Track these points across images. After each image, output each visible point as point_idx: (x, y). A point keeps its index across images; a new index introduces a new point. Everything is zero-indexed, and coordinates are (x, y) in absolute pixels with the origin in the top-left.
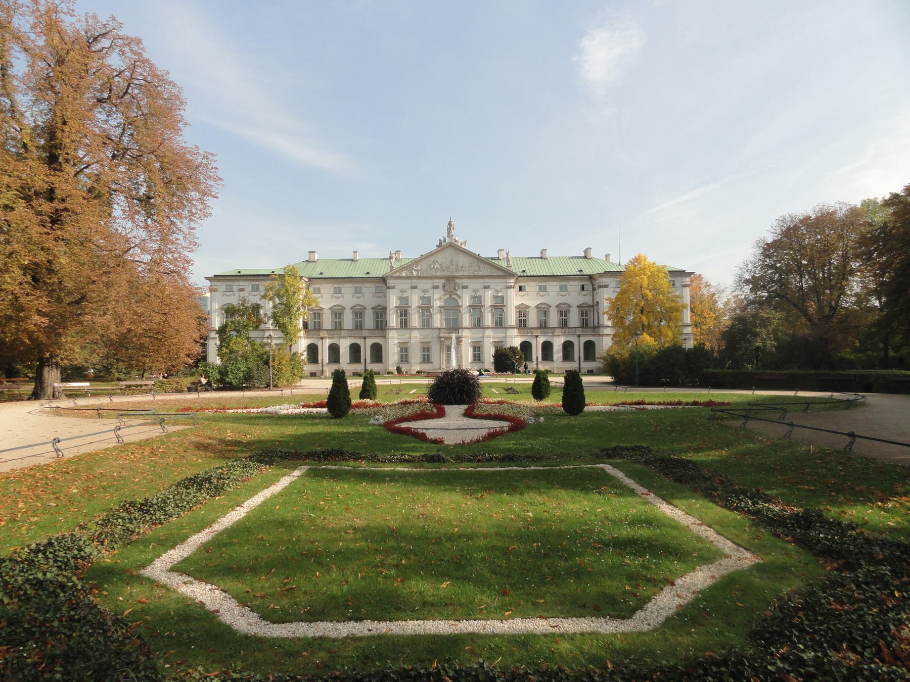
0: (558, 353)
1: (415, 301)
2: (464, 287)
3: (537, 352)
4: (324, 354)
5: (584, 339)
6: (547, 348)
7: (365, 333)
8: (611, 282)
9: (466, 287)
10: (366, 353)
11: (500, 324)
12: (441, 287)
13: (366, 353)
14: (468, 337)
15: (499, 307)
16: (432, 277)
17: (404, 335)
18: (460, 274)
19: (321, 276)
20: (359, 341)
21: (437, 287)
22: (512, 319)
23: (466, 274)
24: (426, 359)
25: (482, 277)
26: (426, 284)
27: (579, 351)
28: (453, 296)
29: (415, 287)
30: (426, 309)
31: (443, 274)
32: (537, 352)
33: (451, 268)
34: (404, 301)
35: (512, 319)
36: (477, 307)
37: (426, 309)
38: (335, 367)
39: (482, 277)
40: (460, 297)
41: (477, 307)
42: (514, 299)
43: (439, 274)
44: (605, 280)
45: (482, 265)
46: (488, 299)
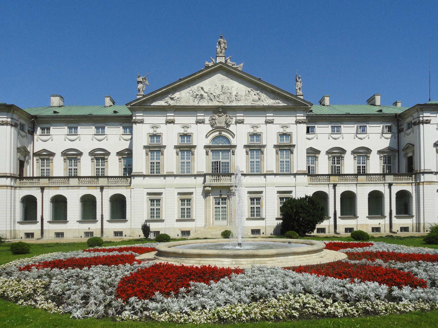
0: (362, 205)
2: (237, 122)
3: (334, 205)
4: (45, 209)
5: (396, 189)
9: (242, 122)
10: (104, 208)
12: (207, 121)
13: (104, 208)
14: (245, 186)
15: (285, 148)
17: (155, 183)
18: (234, 104)
20: (96, 193)
21: (203, 122)
22: (300, 161)
24: (186, 215)
28: (223, 133)
29: (172, 122)
30: (186, 148)
31: (211, 104)
33: (222, 97)
36: (255, 148)
37: (186, 148)
38: (59, 227)
40: (233, 135)
41: (255, 148)
43: (204, 103)
44: (426, 115)
46: (270, 136)
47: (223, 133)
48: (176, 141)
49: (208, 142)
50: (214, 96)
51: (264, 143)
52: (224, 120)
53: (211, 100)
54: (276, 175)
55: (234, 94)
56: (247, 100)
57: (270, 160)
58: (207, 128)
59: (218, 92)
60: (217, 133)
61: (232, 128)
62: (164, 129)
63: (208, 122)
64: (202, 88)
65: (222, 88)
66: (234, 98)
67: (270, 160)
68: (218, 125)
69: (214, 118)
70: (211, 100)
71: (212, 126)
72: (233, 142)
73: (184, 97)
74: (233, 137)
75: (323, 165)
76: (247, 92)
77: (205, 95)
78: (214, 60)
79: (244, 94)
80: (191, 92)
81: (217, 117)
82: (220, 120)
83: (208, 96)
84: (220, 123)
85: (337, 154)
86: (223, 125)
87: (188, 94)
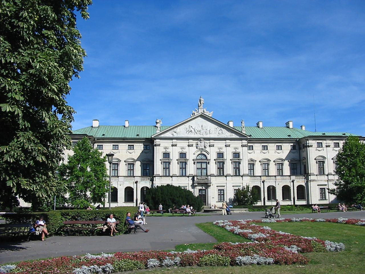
1: (175, 156)
3: (264, 194)
6: (272, 190)
7: (137, 179)
8: (312, 143)
11: (237, 172)
12: (194, 145)
14: (215, 182)
16: (188, 139)
18: (208, 136)
19: (103, 137)
23: (212, 136)
25: (225, 139)
26: (185, 144)
27: (294, 193)
28: (203, 152)
32: (264, 194)
33: (202, 131)
34: (166, 155)
35: (244, 168)
39: (225, 139)
42: (246, 156)
45: (224, 130)
47: (203, 152)
48: (177, 157)
49: (194, 157)
50: (198, 131)
51: (225, 158)
52: (204, 145)
53: (196, 133)
54: (232, 176)
55: (209, 130)
56: (215, 133)
57: (229, 168)
58: (193, 149)
59: (200, 129)
60: (199, 152)
61: (208, 149)
62: (170, 150)
63: (195, 146)
64: (191, 127)
65: (202, 126)
66: (208, 132)
67: (229, 168)
68: (201, 148)
69: (198, 143)
70: (196, 133)
71: (197, 148)
72: (209, 158)
73: (181, 131)
74: (208, 154)
75: (258, 170)
76: (215, 129)
77: (193, 130)
78: (197, 110)
79: (214, 130)
80: (185, 128)
81: (200, 143)
82: (201, 145)
83: (195, 131)
84: (201, 146)
85: (266, 164)
86: (203, 148)
87: (184, 130)
